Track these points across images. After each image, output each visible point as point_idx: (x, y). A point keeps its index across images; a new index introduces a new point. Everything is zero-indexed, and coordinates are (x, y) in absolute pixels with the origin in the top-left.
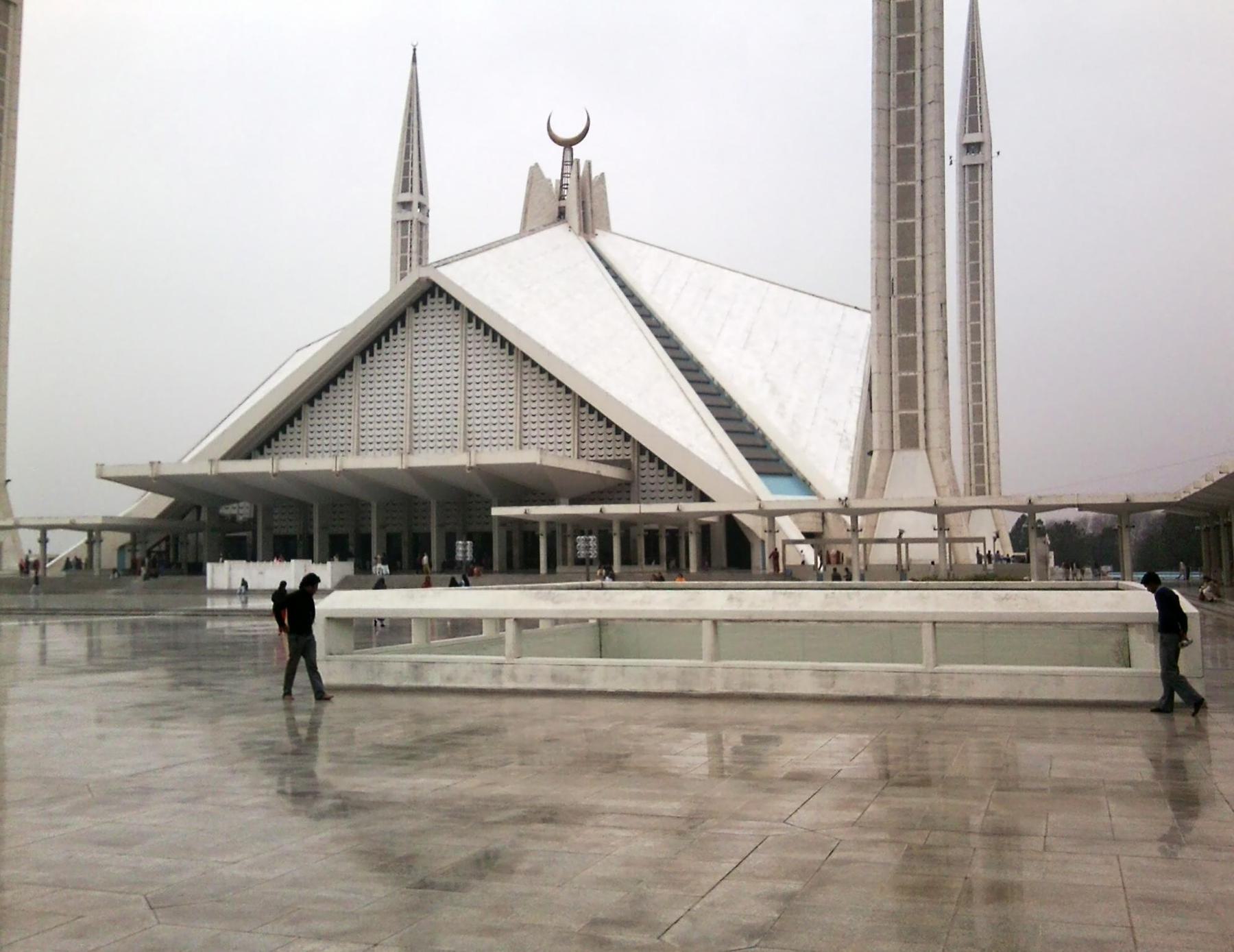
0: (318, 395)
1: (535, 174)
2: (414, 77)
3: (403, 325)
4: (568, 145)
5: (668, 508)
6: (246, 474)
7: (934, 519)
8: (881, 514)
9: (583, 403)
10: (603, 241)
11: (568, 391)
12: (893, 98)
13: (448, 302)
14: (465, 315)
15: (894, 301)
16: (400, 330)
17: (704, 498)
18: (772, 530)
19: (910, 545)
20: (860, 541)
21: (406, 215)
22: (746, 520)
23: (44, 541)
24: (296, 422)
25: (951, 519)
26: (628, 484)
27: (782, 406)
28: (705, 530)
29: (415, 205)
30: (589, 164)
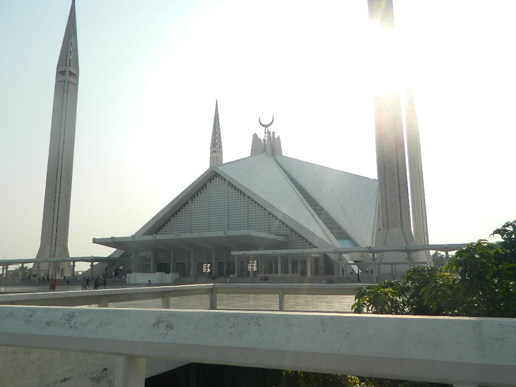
1: (255, 136)
2: (217, 111)
3: (206, 188)
4: (266, 126)
7: (406, 254)
8: (384, 253)
9: (270, 214)
11: (265, 209)
13: (222, 179)
14: (228, 183)
16: (205, 189)
18: (341, 259)
19: (397, 265)
20: (376, 264)
22: (332, 256)
23: (74, 266)
24: (169, 223)
25: (413, 254)
26: (287, 243)
28: (317, 259)
30: (274, 133)
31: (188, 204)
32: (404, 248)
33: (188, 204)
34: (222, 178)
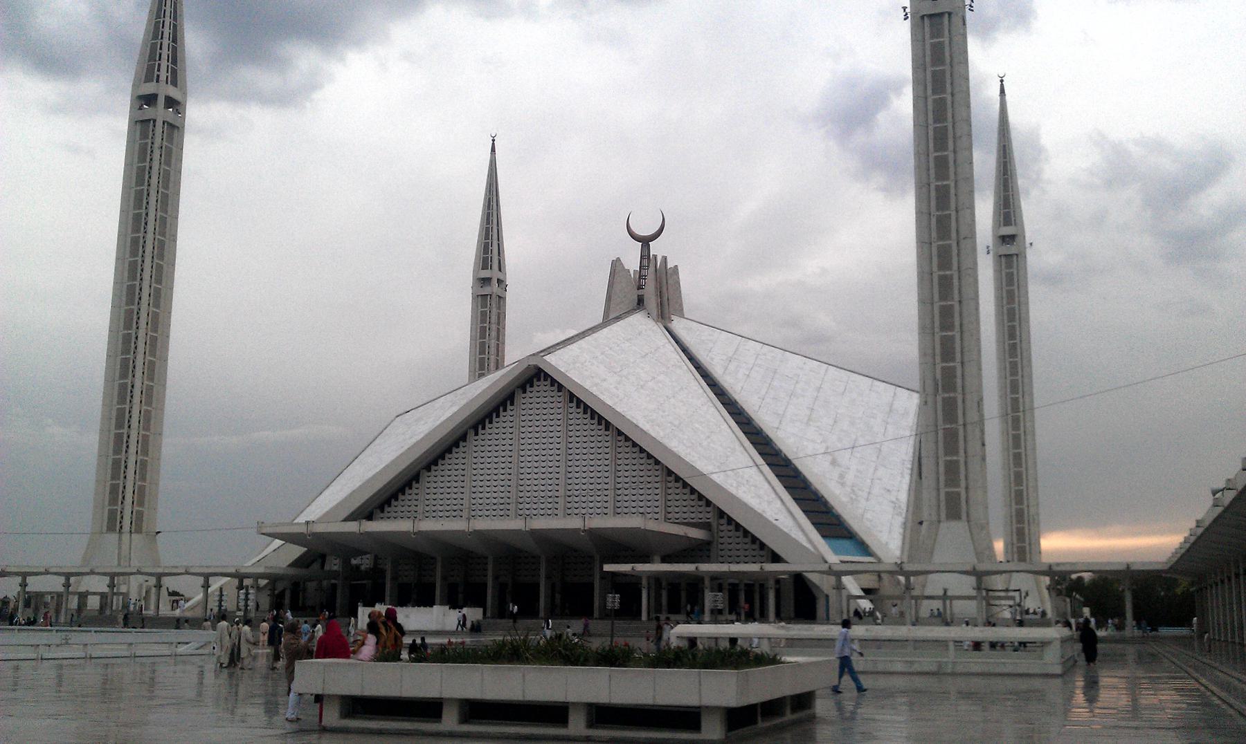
0: (435, 462)
1: (616, 265)
3: (512, 404)
4: (645, 241)
5: (754, 567)
6: (384, 533)
7: (972, 580)
8: (931, 576)
10: (678, 325)
11: (657, 462)
12: (934, 234)
15: (939, 399)
16: (509, 407)
17: (776, 558)
18: (839, 587)
19: (954, 602)
20: (912, 597)
21: (487, 290)
22: (814, 578)
26: (709, 543)
27: (842, 476)
29: (495, 282)
30: (665, 259)
31: (465, 441)
32: (968, 568)
33: (465, 441)
34: (553, 381)
